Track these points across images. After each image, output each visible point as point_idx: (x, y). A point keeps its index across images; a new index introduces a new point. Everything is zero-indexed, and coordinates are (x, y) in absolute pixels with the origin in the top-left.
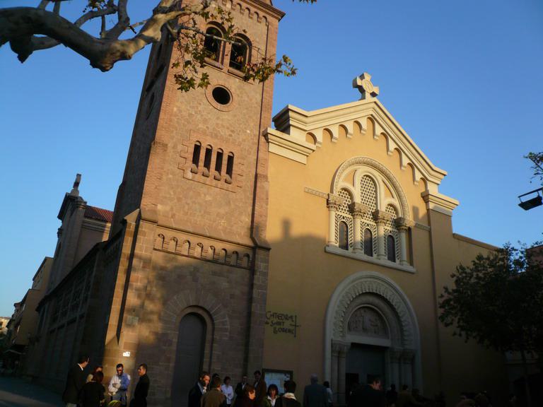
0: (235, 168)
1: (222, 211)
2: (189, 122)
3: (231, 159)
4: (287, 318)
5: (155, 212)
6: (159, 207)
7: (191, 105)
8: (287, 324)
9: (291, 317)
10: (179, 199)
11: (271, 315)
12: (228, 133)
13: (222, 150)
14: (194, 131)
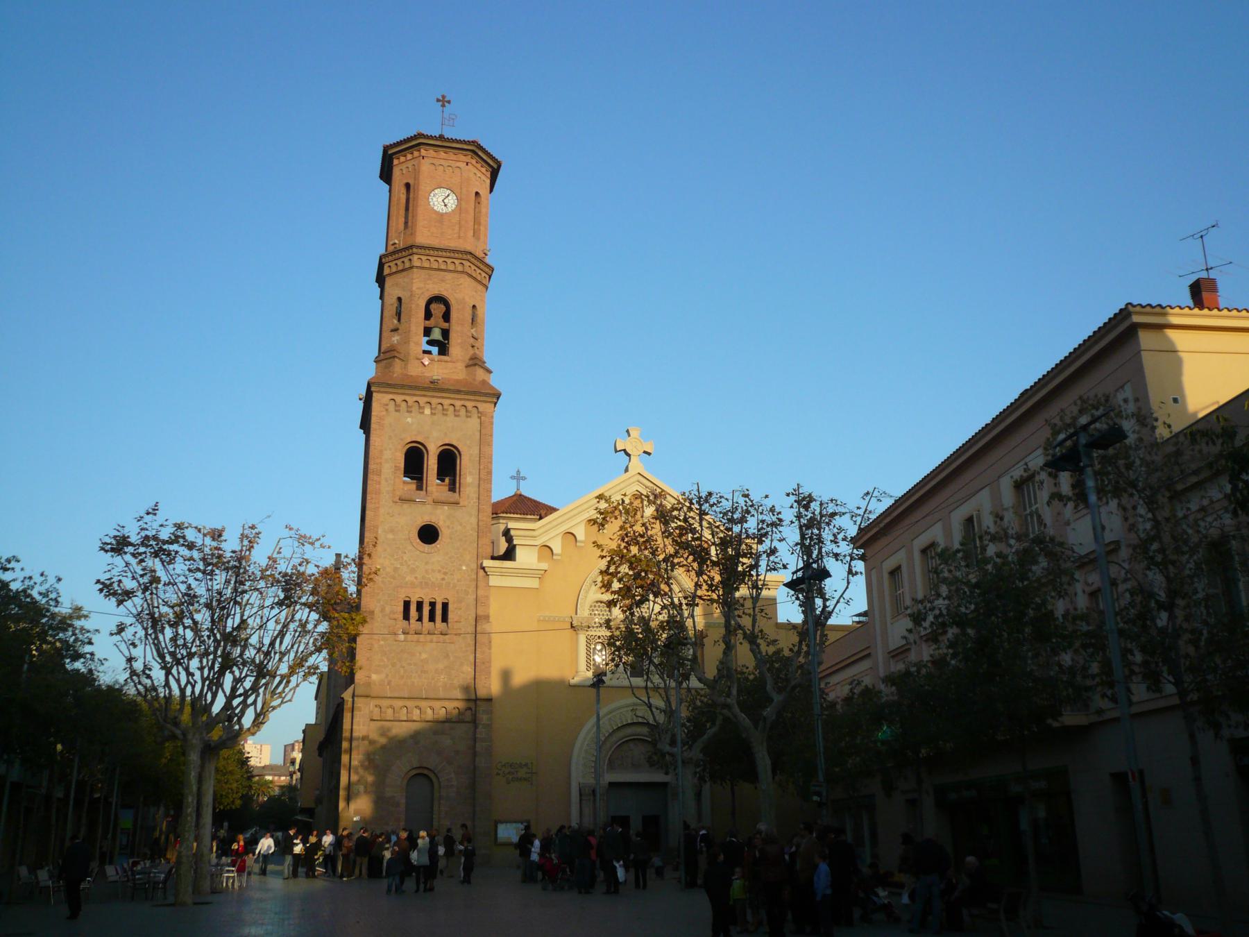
0: (451, 616)
1: (441, 666)
2: (394, 578)
3: (445, 606)
4: (521, 766)
5: (368, 684)
6: (374, 677)
7: (396, 557)
8: (522, 773)
9: (526, 765)
10: (394, 665)
11: (502, 766)
12: (439, 576)
13: (435, 599)
14: (401, 587)
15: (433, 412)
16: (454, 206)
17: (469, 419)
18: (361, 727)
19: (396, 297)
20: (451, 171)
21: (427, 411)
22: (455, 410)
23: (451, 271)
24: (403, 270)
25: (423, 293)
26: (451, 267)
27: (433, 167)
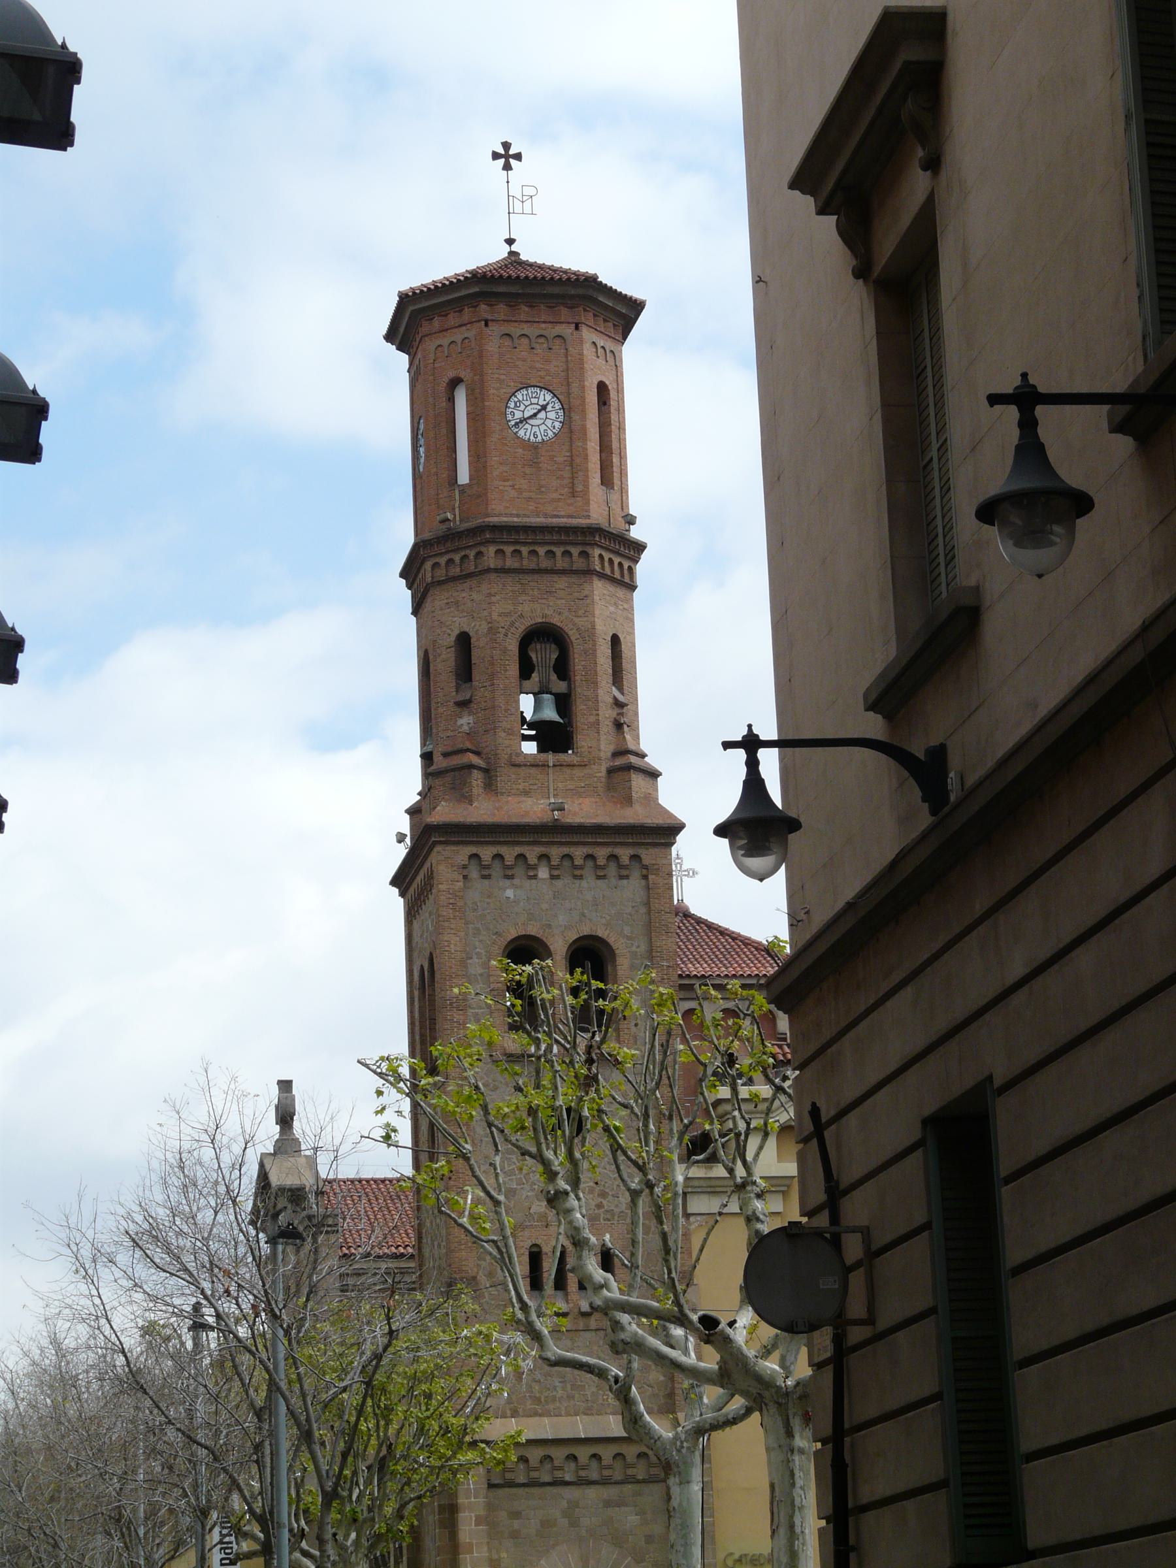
15: (556, 873)
16: (557, 425)
17: (625, 882)
18: (473, 1500)
19: (457, 632)
20: (545, 345)
21: (543, 873)
22: (597, 867)
23: (563, 572)
24: (470, 575)
25: (512, 624)
26: (561, 563)
27: (507, 342)
